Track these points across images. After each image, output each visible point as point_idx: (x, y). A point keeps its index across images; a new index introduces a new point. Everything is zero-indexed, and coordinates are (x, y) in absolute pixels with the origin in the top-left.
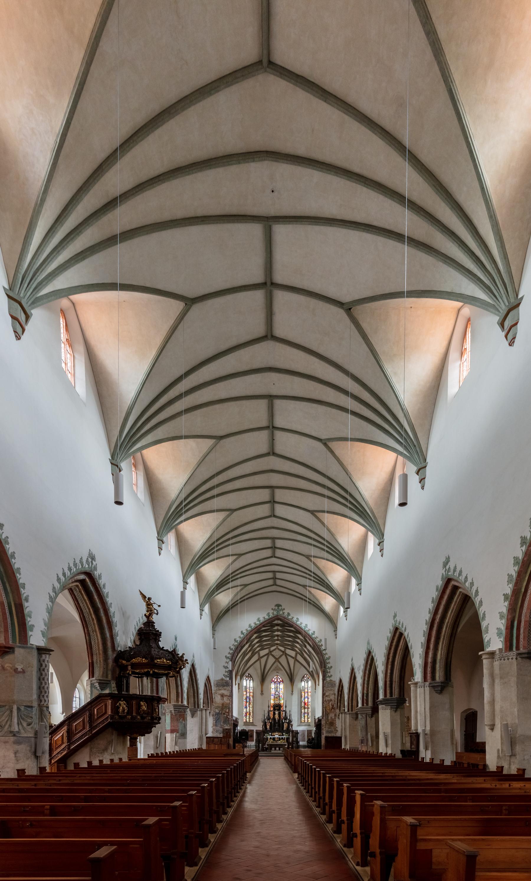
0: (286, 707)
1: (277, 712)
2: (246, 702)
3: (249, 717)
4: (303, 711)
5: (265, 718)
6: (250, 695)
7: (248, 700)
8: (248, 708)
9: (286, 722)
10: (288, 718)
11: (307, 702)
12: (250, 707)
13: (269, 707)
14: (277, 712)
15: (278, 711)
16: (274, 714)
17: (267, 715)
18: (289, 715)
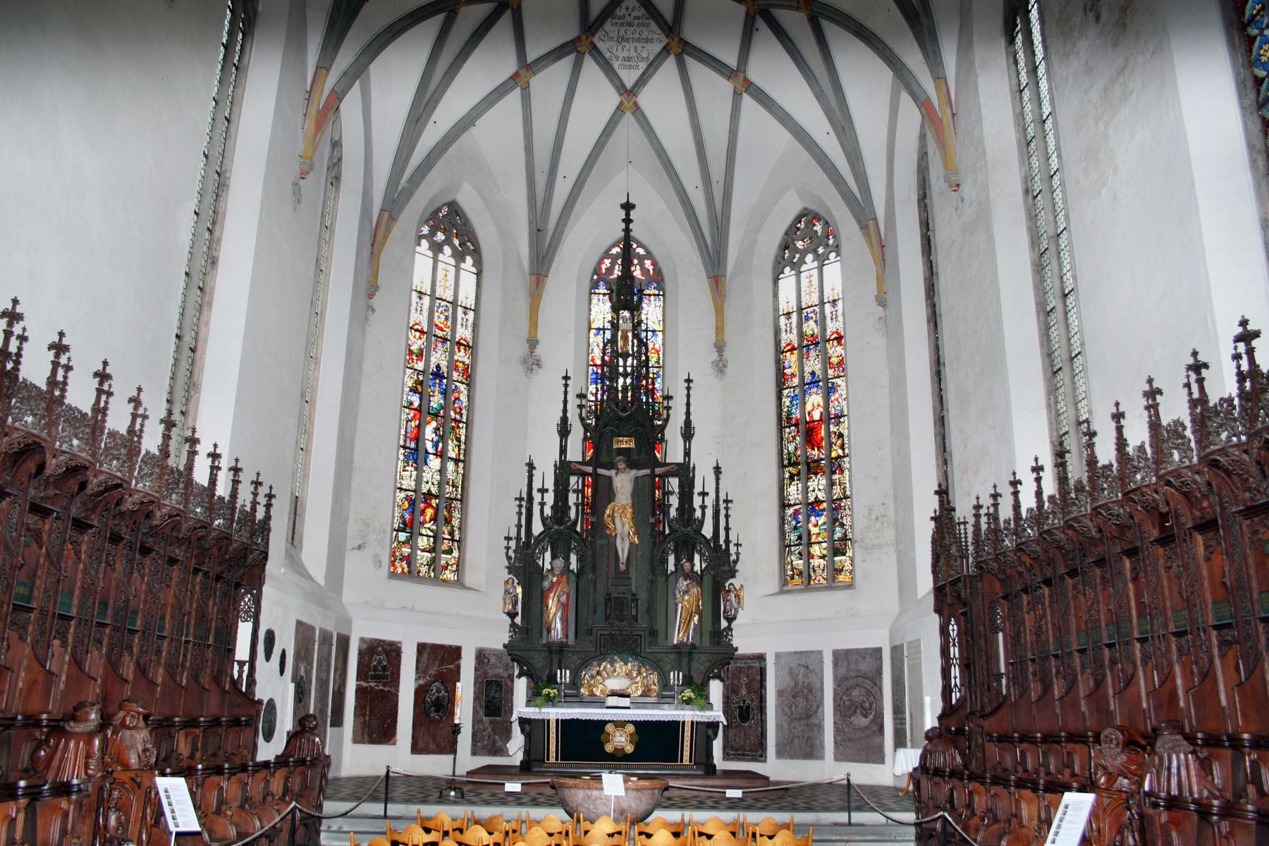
0: (688, 433)
1: (623, 482)
2: (422, 412)
3: (436, 536)
4: (794, 492)
5: (538, 528)
6: (453, 365)
7: (436, 401)
8: (435, 463)
9: (691, 575)
10: (707, 531)
11: (816, 416)
12: (441, 455)
13: (564, 430)
14: (623, 482)
15: (632, 465)
16: (602, 493)
17: (550, 498)
18: (709, 501)
